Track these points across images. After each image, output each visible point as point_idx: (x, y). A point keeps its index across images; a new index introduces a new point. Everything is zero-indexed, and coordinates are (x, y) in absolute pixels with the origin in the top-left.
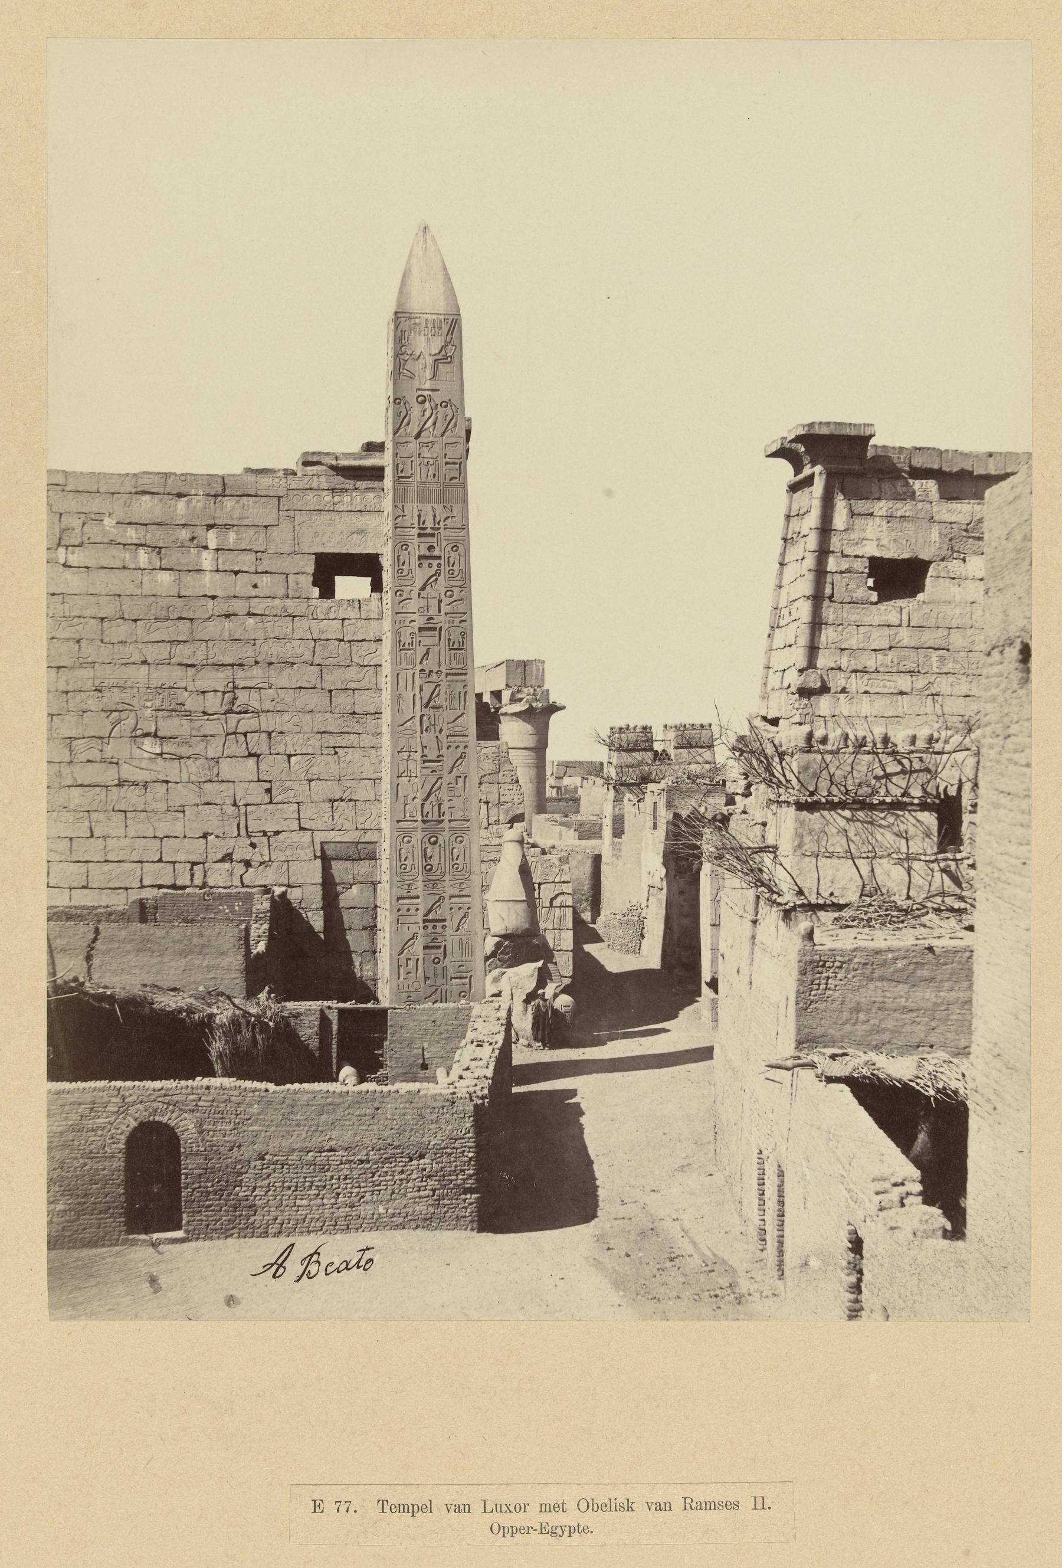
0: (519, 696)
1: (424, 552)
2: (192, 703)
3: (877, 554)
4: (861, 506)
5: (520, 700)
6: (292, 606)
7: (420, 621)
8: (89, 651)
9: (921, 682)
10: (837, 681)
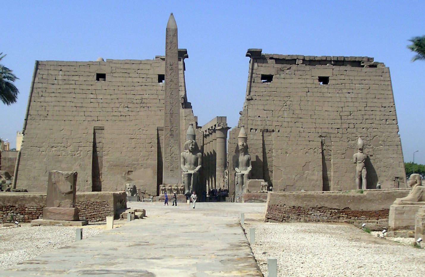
0: (220, 125)
1: (171, 68)
2: (135, 101)
3: (263, 74)
4: (259, 64)
5: (220, 126)
6: (153, 84)
7: (170, 80)
8: (116, 92)
9: (271, 98)
10: (254, 98)
